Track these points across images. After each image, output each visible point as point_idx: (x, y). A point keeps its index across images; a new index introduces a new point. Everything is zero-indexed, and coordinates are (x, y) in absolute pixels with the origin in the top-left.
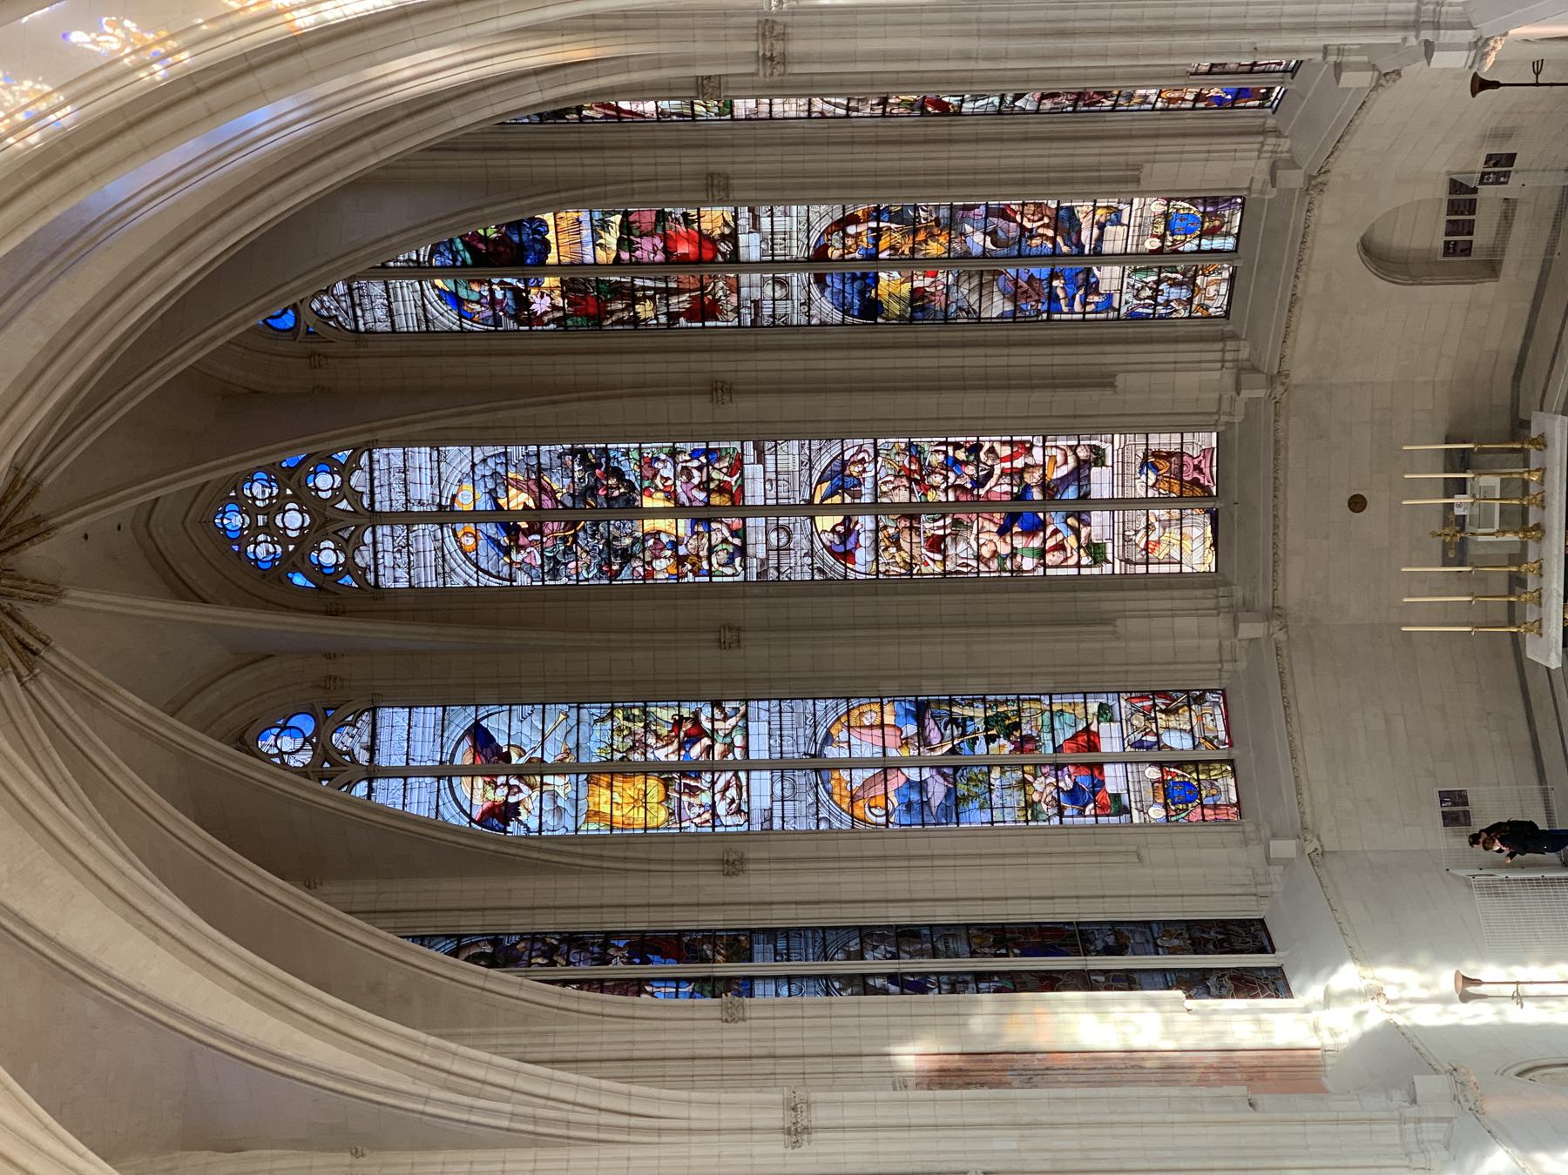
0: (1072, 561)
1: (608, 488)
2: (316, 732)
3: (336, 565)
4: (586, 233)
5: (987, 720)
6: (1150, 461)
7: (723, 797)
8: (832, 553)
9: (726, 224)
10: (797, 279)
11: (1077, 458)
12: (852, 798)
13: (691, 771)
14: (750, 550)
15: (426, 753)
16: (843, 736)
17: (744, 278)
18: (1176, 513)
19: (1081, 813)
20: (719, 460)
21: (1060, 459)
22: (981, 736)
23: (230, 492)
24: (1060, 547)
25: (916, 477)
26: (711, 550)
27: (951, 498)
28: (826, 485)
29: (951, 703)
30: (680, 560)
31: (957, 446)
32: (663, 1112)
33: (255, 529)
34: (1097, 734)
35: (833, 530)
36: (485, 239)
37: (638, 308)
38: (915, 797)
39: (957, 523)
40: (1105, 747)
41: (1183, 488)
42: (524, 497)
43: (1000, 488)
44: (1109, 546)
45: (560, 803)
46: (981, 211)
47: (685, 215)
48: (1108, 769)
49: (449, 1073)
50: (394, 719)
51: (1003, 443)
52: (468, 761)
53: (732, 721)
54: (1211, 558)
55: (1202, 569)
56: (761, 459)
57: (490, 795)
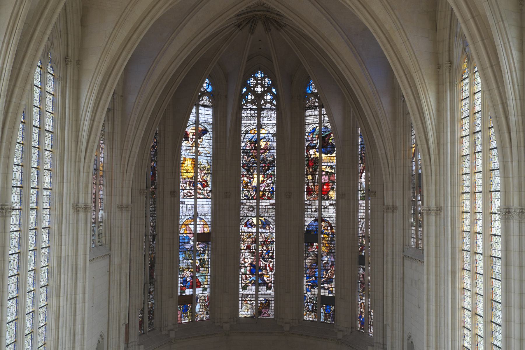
1: (265, 166)
2: (207, 92)
3: (248, 99)
4: (329, 164)
5: (204, 259)
6: (268, 302)
7: (188, 192)
8: (247, 221)
9: (331, 197)
10: (317, 214)
11: (268, 283)
12: (186, 225)
13: (195, 184)
14: (248, 201)
15: (202, 119)
16: (202, 223)
17: (317, 201)
18: (254, 307)
19: (181, 283)
20: (271, 194)
22: (200, 258)
23: (268, 74)
25: (266, 243)
26: (249, 191)
27: (260, 252)
28: (264, 220)
29: (208, 250)
30: (246, 184)
31: (273, 253)
32: (128, 173)
33: (257, 80)
34: (200, 287)
35: (252, 222)
36: (329, 139)
37: (310, 176)
38: (186, 241)
39: (253, 253)
40: (197, 289)
41: (261, 308)
42: (263, 146)
43: (262, 263)
45: (188, 151)
46: (333, 260)
47: (334, 188)
48: (191, 290)
49: (141, 120)
50: (210, 111)
51: (273, 265)
52: (200, 129)
53: (206, 195)
54: (242, 316)
55: (240, 314)
56: (271, 204)
57: (191, 134)
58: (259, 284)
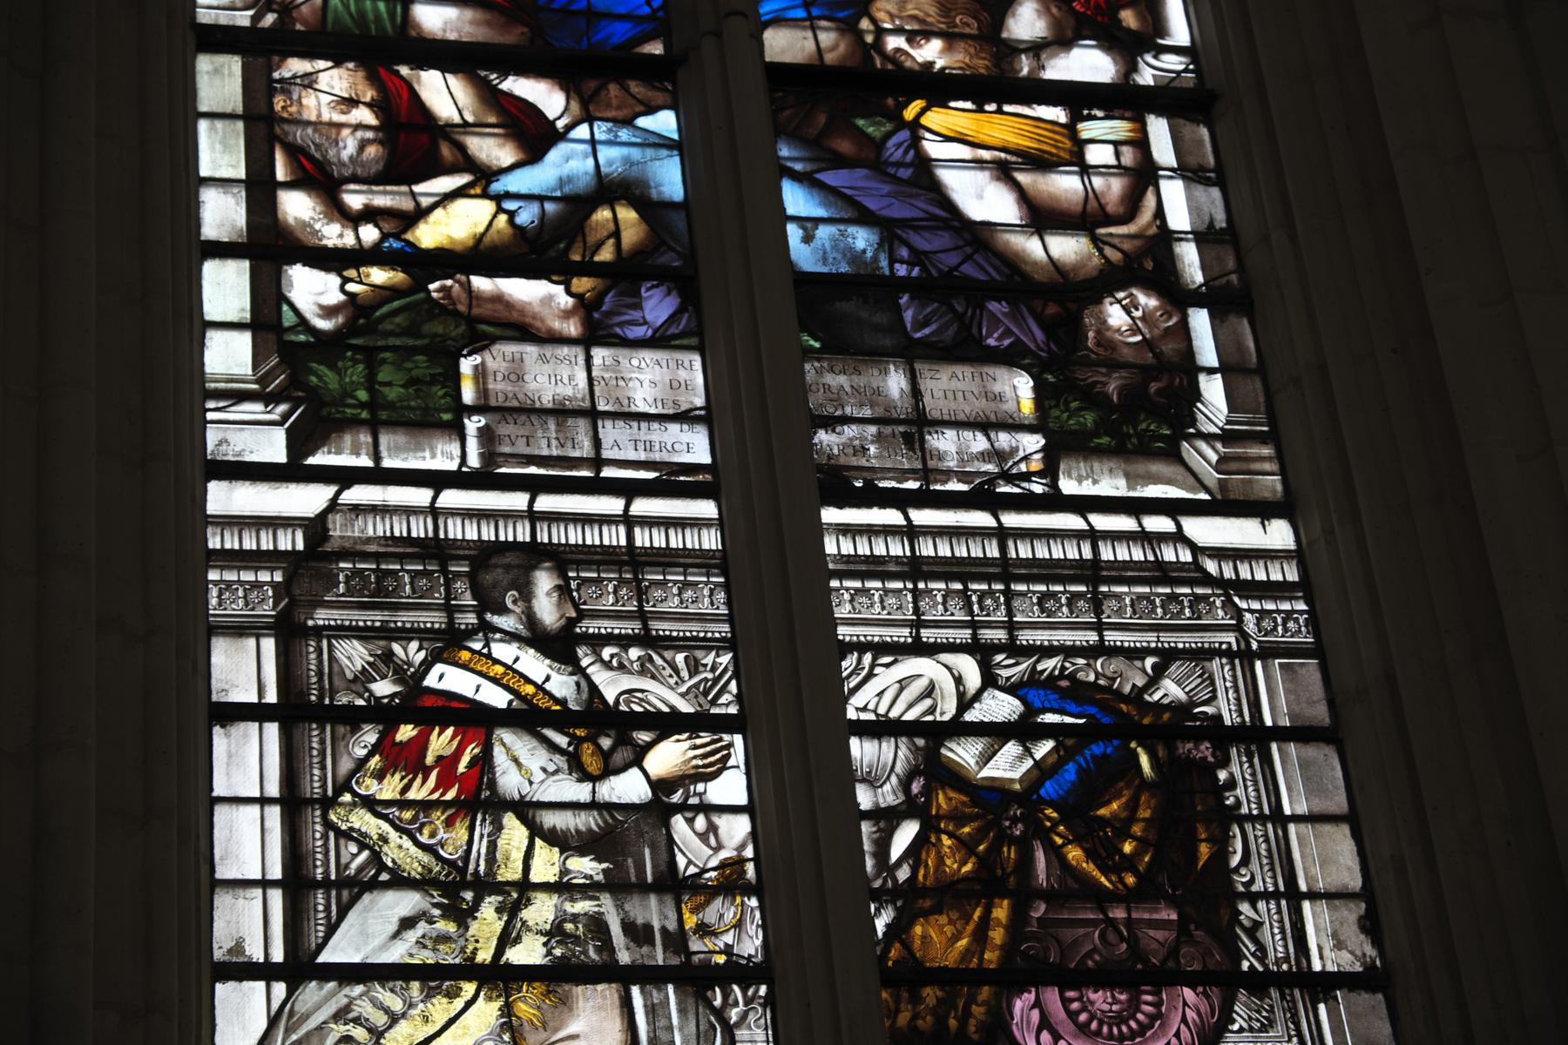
0: (297, 206)
6: (1137, 782)
21: (1065, 185)
24: (414, 144)
44: (442, 457)
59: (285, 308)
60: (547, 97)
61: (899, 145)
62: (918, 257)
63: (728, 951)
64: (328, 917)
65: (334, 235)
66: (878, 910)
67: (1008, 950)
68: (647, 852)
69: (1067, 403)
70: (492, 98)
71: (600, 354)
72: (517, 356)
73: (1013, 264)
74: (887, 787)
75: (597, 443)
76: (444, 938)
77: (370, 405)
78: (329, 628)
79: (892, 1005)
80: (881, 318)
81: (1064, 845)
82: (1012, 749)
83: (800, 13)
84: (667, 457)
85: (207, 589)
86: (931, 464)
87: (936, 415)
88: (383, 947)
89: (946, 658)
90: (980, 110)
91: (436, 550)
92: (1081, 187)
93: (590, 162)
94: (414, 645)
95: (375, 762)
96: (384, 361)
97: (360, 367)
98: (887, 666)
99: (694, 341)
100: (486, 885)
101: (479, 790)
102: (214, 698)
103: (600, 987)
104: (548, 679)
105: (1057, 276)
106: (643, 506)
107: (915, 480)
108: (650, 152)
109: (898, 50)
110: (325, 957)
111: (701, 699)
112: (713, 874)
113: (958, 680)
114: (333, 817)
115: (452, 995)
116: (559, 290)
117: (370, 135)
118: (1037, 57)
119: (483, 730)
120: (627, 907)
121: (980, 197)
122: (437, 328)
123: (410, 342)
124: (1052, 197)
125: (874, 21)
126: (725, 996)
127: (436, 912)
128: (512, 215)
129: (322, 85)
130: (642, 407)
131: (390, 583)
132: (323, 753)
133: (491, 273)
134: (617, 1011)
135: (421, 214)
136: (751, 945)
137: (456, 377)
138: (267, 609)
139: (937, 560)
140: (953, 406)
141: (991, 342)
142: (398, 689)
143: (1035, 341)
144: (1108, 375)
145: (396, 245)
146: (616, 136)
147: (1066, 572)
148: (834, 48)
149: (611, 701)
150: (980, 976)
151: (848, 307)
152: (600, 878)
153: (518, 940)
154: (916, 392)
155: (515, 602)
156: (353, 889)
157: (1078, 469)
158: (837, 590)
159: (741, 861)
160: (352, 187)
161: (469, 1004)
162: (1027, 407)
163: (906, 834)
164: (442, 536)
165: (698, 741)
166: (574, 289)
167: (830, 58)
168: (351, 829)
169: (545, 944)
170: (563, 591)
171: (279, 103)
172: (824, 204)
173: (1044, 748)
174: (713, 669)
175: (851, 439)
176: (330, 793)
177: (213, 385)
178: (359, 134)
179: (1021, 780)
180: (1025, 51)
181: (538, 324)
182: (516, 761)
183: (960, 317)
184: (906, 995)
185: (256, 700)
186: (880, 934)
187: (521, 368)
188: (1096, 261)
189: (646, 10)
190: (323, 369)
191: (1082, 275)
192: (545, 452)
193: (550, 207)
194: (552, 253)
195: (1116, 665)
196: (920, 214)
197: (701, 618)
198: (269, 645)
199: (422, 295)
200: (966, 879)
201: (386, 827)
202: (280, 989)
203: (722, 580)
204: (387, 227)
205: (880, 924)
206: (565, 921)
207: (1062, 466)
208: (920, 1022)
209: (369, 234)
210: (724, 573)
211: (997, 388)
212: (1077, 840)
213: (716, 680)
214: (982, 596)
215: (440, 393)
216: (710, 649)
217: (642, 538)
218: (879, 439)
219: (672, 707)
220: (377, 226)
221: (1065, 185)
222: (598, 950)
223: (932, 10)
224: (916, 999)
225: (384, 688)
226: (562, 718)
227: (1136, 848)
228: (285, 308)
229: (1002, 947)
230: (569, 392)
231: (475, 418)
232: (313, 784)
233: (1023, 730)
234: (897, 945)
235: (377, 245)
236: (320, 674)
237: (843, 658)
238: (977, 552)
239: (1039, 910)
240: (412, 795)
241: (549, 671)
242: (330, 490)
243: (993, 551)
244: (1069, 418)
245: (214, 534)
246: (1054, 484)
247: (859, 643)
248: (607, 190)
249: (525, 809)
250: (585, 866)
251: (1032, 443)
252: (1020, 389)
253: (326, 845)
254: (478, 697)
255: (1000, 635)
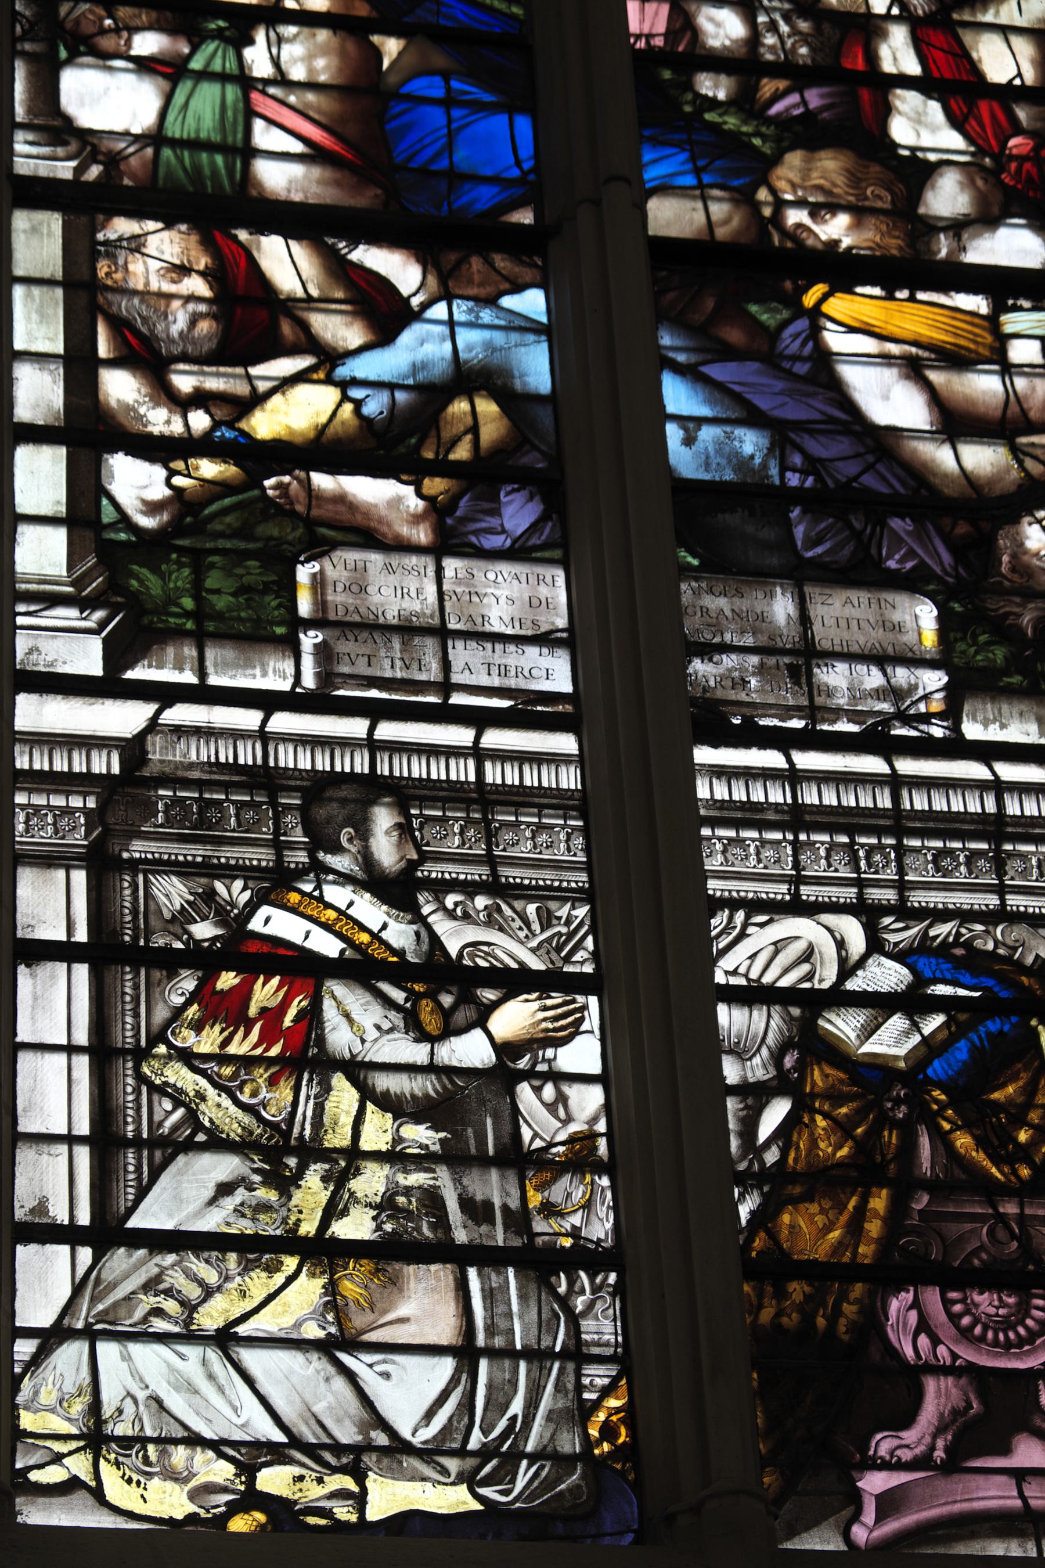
0: (120, 387)
21: (984, 386)
24: (251, 322)
44: (273, 675)
58: (697, 505)
59: (105, 502)
60: (400, 270)
61: (796, 336)
62: (812, 465)
63: (574, 1232)
64: (139, 1179)
65: (160, 421)
66: (742, 1195)
67: (886, 1243)
68: (489, 1121)
69: (975, 637)
70: (341, 270)
71: (452, 566)
72: (360, 565)
73: (920, 475)
74: (757, 1060)
75: (446, 666)
76: (263, 1207)
77: (198, 616)
78: (146, 861)
79: (754, 1299)
80: (768, 534)
81: (951, 1131)
82: (897, 1022)
83: (690, 180)
84: (523, 684)
85: (13, 814)
86: (819, 701)
87: (826, 645)
88: (198, 1214)
89: (828, 918)
90: (890, 297)
91: (265, 779)
92: (1001, 388)
93: (448, 346)
94: (238, 884)
95: (193, 1011)
96: (212, 566)
97: (186, 572)
98: (762, 925)
99: (557, 554)
100: (312, 1151)
101: (306, 1047)
102: (20, 934)
103: (433, 1267)
104: (385, 927)
105: (969, 491)
106: (495, 738)
107: (800, 718)
108: (515, 337)
109: (799, 226)
110: (135, 1222)
111: (554, 956)
112: (561, 1149)
113: (841, 944)
114: (146, 1070)
115: (272, 1269)
116: (410, 490)
117: (202, 308)
118: (958, 236)
119: (311, 982)
120: (465, 1181)
121: (886, 397)
122: (271, 529)
123: (243, 545)
124: (970, 401)
125: (773, 191)
126: (571, 1283)
127: (257, 1178)
128: (358, 404)
129: (151, 248)
130: (497, 627)
131: (213, 814)
132: (136, 1000)
133: (334, 469)
134: (451, 1294)
135: (256, 400)
136: (600, 1228)
137: (292, 586)
138: (78, 838)
139: (821, 809)
140: (846, 635)
141: (892, 564)
142: (219, 932)
143: (941, 563)
144: (1023, 605)
145: (229, 434)
146: (477, 317)
147: (966, 827)
148: (727, 221)
149: (453, 952)
150: (854, 1272)
151: (732, 519)
152: (436, 1148)
153: (344, 1213)
154: (804, 619)
155: (350, 840)
156: (166, 1149)
157: (985, 710)
158: (709, 839)
159: (591, 1136)
160: (181, 366)
161: (290, 1280)
162: (930, 639)
163: (775, 1113)
164: (272, 764)
165: (549, 1002)
166: (425, 491)
167: (721, 233)
168: (166, 1084)
169: (374, 1218)
170: (404, 830)
171: (103, 268)
172: (710, 402)
173: (933, 1023)
174: (568, 923)
175: (729, 670)
176: (143, 1043)
177: (24, 586)
178: (191, 307)
179: (906, 1058)
180: (944, 229)
181: (384, 529)
182: (347, 1016)
183: (857, 535)
184: (769, 1289)
185: (64, 939)
186: (744, 1222)
187: (364, 579)
188: (1015, 474)
189: (515, 173)
190: (144, 571)
191: (997, 491)
192: (388, 674)
193: (401, 396)
194: (402, 449)
195: (1019, 932)
196: (817, 416)
197: (556, 865)
198: (79, 877)
199: (256, 492)
200: (841, 1164)
201: (203, 1083)
202: (85, 1255)
203: (580, 823)
204: (219, 414)
205: (744, 1211)
206: (396, 1193)
207: (966, 708)
208: (785, 1320)
209: (200, 421)
210: (583, 816)
211: (896, 617)
212: (967, 1126)
213: (571, 935)
214: (871, 850)
215: (274, 604)
216: (565, 900)
217: (493, 774)
218: (761, 670)
219: (521, 963)
220: (208, 412)
221: (984, 386)
222: (433, 1227)
223: (840, 180)
224: (781, 1294)
225: (204, 930)
226: (399, 970)
227: (1032, 1137)
228: (105, 502)
229: (878, 1241)
230: (417, 606)
231: (311, 633)
232: (124, 1035)
233: (911, 1002)
234: (762, 1234)
235: (208, 434)
236: (135, 912)
237: (713, 915)
238: (866, 801)
239: (922, 1201)
240: (233, 1049)
241: (386, 918)
242: (150, 709)
243: (885, 801)
244: (977, 653)
245: (22, 753)
246: (956, 728)
247: (731, 898)
248: (466, 378)
249: (357, 1070)
250: (420, 1135)
251: (934, 680)
252: (923, 619)
253: (137, 1101)
254: (308, 944)
255: (889, 895)
